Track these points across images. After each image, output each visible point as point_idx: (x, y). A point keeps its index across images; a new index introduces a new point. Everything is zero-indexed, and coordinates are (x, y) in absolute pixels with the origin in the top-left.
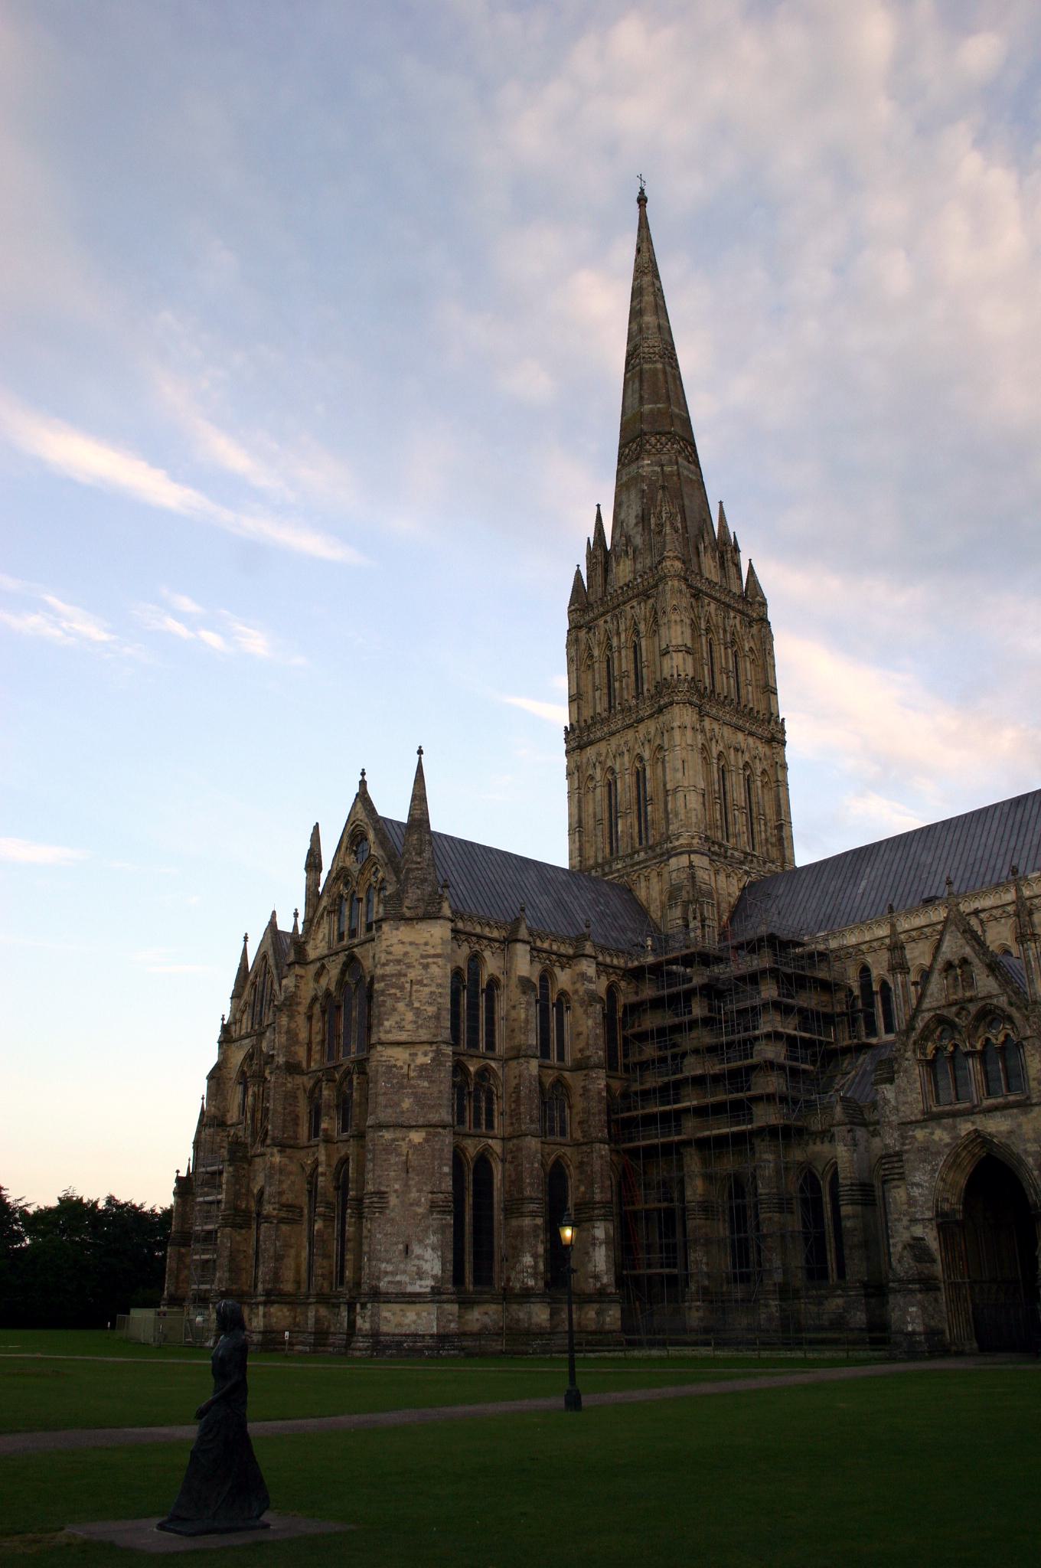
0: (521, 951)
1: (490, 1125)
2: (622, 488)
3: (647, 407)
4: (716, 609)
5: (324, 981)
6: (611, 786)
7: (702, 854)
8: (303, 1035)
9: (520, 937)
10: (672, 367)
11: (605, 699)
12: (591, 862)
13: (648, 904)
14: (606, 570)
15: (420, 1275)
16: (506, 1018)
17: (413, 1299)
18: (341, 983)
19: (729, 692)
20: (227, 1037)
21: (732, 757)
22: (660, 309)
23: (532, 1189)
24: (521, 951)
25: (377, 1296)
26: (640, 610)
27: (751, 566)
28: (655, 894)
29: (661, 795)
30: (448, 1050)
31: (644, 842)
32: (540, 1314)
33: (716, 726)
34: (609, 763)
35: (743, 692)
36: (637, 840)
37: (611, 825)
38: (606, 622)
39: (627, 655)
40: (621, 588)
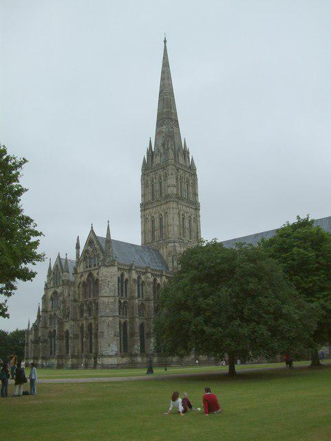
0: (134, 272)
1: (126, 315)
2: (158, 133)
3: (165, 110)
5: (83, 279)
6: (153, 221)
8: (77, 292)
14: (152, 158)
15: (112, 351)
16: (130, 288)
17: (111, 356)
18: (88, 280)
20: (47, 288)
22: (169, 78)
23: (137, 330)
24: (134, 272)
25: (102, 356)
26: (161, 172)
30: (117, 298)
32: (139, 359)
39: (158, 185)
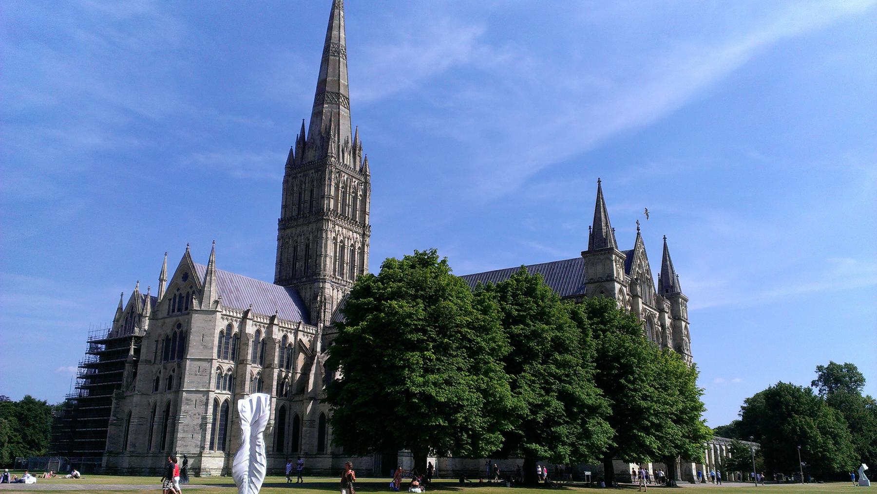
4: (347, 179)
7: (328, 283)
9: (248, 317)
10: (343, 59)
11: (297, 209)
12: (284, 278)
13: (305, 298)
14: (303, 152)
19: (348, 214)
21: (346, 242)
27: (366, 157)
28: (308, 296)
29: (315, 257)
31: (306, 274)
33: (340, 229)
34: (295, 238)
35: (355, 213)
36: (303, 272)
37: (293, 265)
38: (300, 176)
40: (309, 163)
